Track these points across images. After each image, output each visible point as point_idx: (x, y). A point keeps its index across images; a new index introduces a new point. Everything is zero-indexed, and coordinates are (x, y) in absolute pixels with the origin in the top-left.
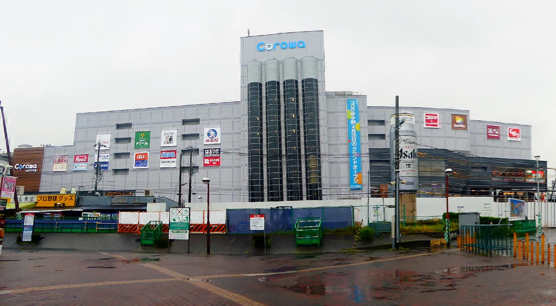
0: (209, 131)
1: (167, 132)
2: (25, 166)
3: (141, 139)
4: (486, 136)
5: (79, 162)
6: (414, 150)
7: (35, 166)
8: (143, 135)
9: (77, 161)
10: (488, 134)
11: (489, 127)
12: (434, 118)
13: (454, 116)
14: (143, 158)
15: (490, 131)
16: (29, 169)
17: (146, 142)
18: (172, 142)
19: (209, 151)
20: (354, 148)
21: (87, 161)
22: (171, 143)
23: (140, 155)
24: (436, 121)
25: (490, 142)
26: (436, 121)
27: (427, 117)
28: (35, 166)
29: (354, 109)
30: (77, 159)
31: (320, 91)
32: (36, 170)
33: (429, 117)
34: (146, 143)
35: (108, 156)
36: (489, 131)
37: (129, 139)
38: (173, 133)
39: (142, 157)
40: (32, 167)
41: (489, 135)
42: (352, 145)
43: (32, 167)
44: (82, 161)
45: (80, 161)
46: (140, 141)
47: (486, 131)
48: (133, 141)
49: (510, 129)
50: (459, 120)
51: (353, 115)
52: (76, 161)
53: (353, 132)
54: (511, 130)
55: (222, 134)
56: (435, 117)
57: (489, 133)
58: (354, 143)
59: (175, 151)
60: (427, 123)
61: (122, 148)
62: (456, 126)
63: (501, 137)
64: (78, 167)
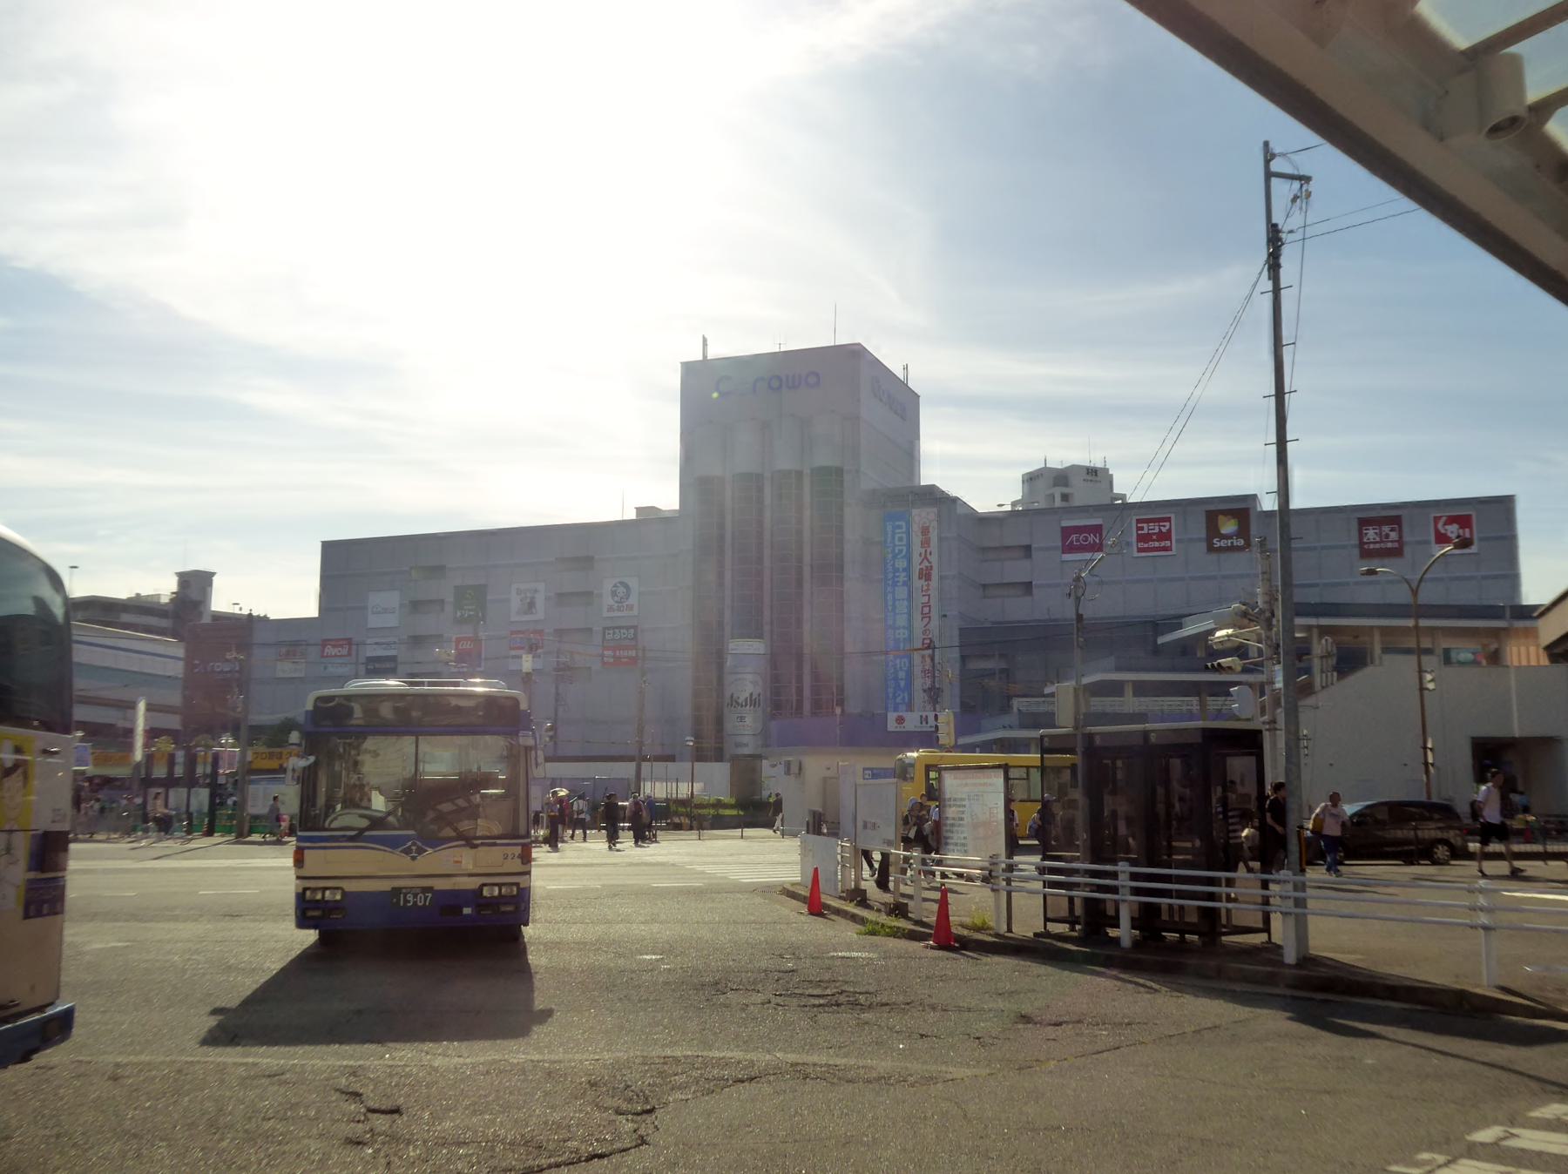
0: (615, 586)
4: (1356, 552)
8: (470, 594)
10: (1362, 544)
11: (1364, 523)
12: (1162, 528)
15: (1371, 534)
16: (221, 672)
18: (534, 611)
19: (614, 633)
22: (532, 613)
24: (1166, 536)
26: (1166, 536)
36: (1366, 534)
41: (1366, 546)
45: (333, 654)
47: (1355, 541)
49: (1437, 520)
50: (1229, 526)
56: (1164, 526)
57: (1365, 540)
62: (1217, 543)
63: (1407, 550)
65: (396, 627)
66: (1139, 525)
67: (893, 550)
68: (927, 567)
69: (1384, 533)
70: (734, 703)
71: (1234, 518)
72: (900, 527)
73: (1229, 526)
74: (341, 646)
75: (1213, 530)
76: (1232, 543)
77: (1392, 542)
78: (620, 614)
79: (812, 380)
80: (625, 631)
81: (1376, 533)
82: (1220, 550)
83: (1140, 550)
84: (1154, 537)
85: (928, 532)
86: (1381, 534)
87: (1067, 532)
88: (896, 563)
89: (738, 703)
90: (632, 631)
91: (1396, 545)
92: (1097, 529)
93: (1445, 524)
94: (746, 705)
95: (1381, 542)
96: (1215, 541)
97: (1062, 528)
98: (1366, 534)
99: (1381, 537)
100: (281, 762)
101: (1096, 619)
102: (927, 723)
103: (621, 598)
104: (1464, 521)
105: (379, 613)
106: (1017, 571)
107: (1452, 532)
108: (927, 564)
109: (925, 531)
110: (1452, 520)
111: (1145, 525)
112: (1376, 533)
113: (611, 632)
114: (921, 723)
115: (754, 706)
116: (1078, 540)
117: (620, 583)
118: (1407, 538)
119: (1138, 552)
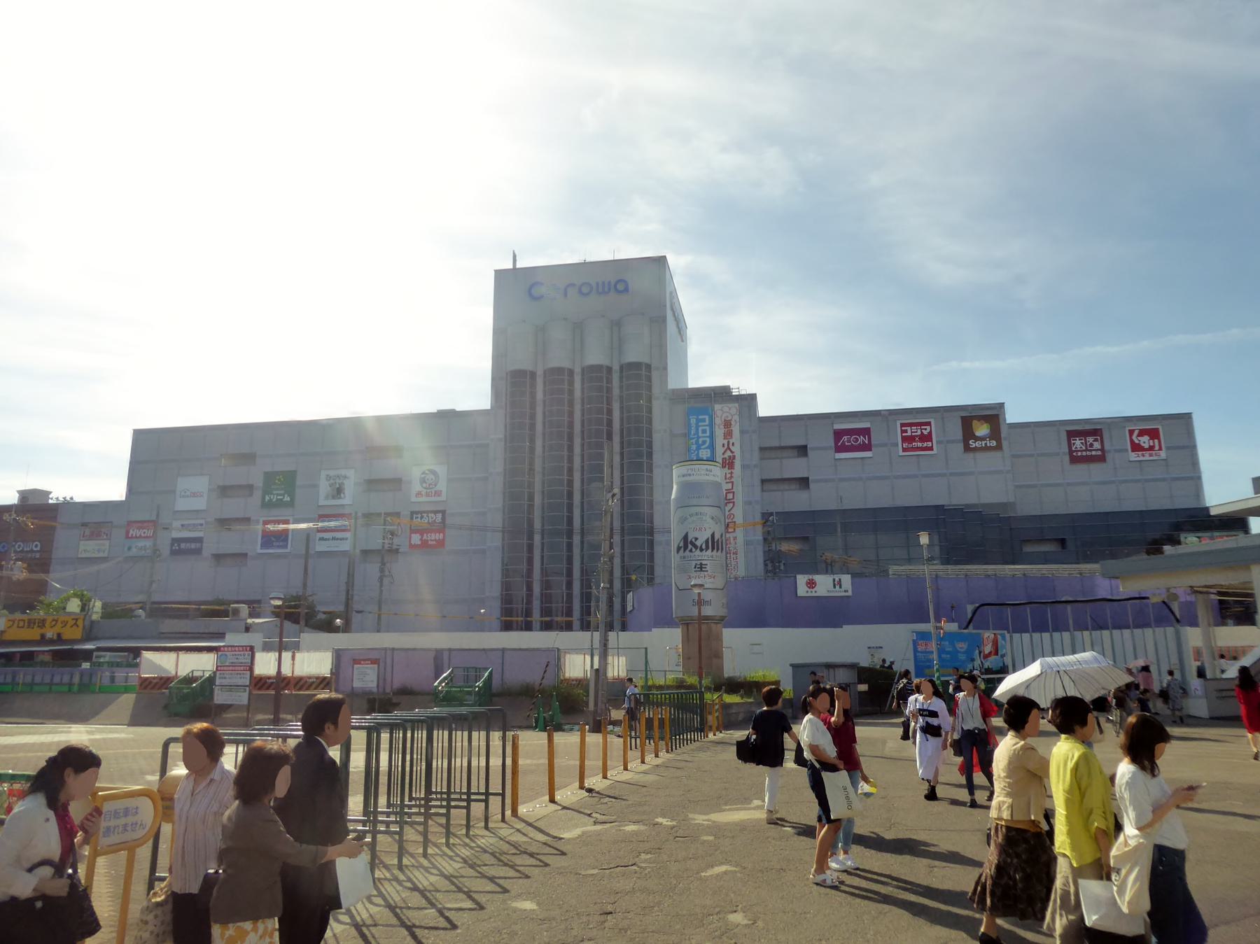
0: (423, 473)
1: (332, 473)
3: (277, 489)
4: (1067, 458)
5: (136, 537)
7: (36, 546)
8: (279, 480)
9: (132, 535)
10: (1071, 452)
11: (1072, 434)
15: (1078, 443)
17: (286, 496)
18: (342, 495)
22: (340, 498)
25: (1081, 470)
26: (928, 438)
27: (906, 431)
28: (36, 546)
30: (133, 530)
31: (656, 390)
32: (38, 556)
34: (287, 499)
35: (201, 525)
37: (250, 488)
38: (345, 477)
45: (138, 535)
46: (275, 492)
48: (258, 494)
50: (982, 430)
52: (130, 536)
56: (926, 429)
61: (233, 507)
65: (204, 510)
66: (903, 428)
67: (697, 443)
68: (730, 457)
70: (690, 546)
72: (704, 420)
75: (968, 434)
76: (986, 444)
79: (620, 287)
80: (433, 515)
82: (976, 449)
83: (904, 450)
85: (731, 424)
86: (1086, 443)
87: (838, 434)
88: (700, 453)
89: (696, 547)
90: (440, 516)
91: (1099, 453)
92: (866, 432)
94: (707, 548)
97: (834, 430)
98: (1074, 444)
99: (1086, 447)
100: (43, 631)
102: (840, 587)
104: (1154, 434)
105: (188, 496)
106: (796, 467)
107: (1144, 443)
108: (731, 454)
109: (727, 424)
110: (1142, 433)
111: (909, 429)
112: (1082, 443)
113: (419, 516)
114: (835, 587)
115: (713, 549)
116: (849, 441)
117: (428, 470)
118: (1107, 447)
119: (903, 451)
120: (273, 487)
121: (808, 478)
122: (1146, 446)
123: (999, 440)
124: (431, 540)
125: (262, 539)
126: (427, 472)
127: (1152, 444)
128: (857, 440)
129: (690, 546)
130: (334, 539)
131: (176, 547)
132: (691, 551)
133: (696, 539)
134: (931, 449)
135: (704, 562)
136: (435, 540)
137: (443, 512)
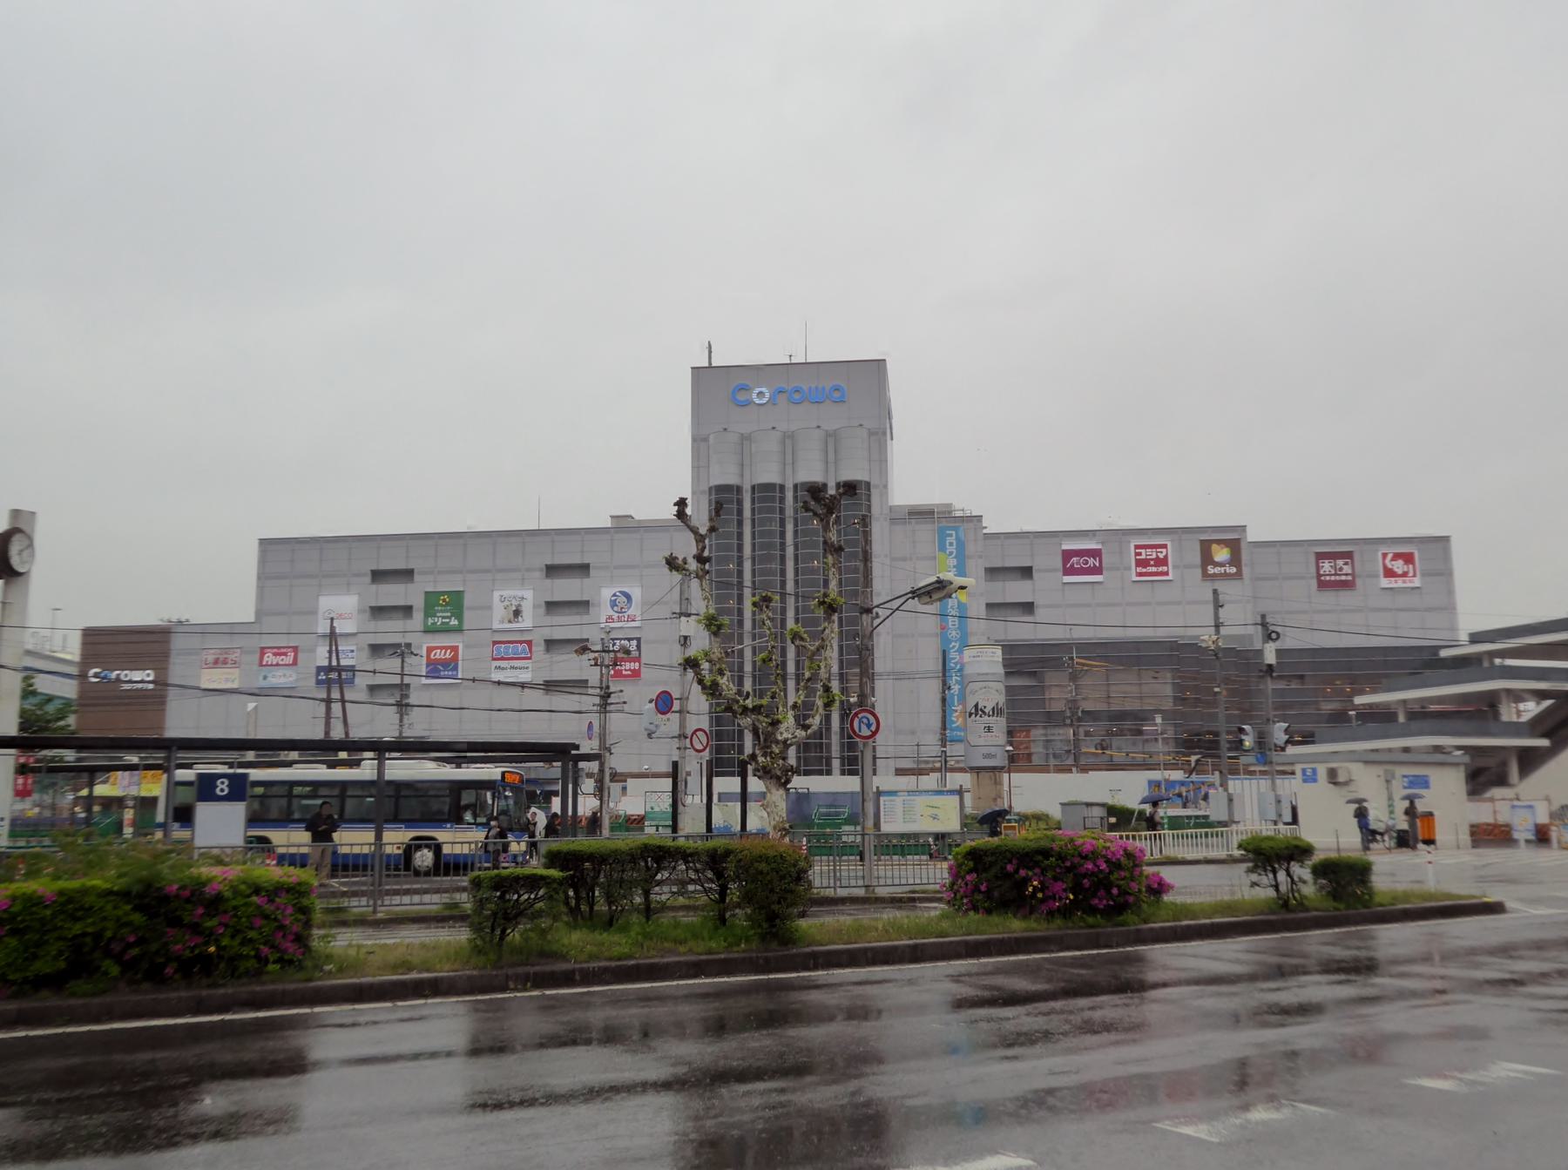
0: (614, 595)
1: (506, 593)
2: (118, 675)
3: (442, 611)
4: (1314, 583)
5: (272, 665)
6: (997, 704)
8: (444, 600)
9: (267, 662)
10: (1319, 575)
11: (1321, 556)
13: (1206, 547)
14: (447, 656)
15: (1327, 566)
16: (130, 682)
20: (953, 644)
21: (295, 663)
22: (518, 622)
23: (439, 651)
24: (1162, 562)
25: (1330, 598)
26: (1162, 562)
27: (1140, 554)
29: (955, 551)
31: (875, 510)
32: (151, 686)
33: (1144, 554)
34: (454, 622)
35: (352, 651)
36: (1323, 567)
37: (407, 610)
39: (445, 654)
40: (141, 677)
41: (1323, 578)
42: (950, 637)
43: (141, 677)
44: (281, 663)
45: (274, 663)
46: (438, 614)
47: (1313, 570)
48: (418, 616)
49: (1385, 555)
50: (1221, 554)
51: (952, 565)
52: (264, 663)
53: (951, 607)
54: (1390, 556)
55: (644, 603)
56: (1162, 552)
57: (1322, 572)
58: (954, 633)
59: (529, 643)
60: (1139, 569)
61: (391, 631)
62: (1211, 570)
63: (1359, 582)
64: (269, 679)
69: (1338, 567)
71: (1227, 547)
73: (1221, 554)
74: (285, 654)
75: (1207, 559)
76: (1225, 570)
77: (1346, 575)
78: (620, 624)
81: (1331, 566)
83: (1140, 574)
84: (1152, 563)
87: (1067, 555)
90: (634, 643)
91: (1350, 578)
92: (1095, 554)
93: (1392, 560)
95: (1336, 574)
96: (1209, 567)
97: (1063, 551)
98: (1323, 567)
99: (1336, 570)
101: (1073, 639)
103: (622, 608)
104: (1408, 558)
106: (1017, 591)
107: (1398, 568)
110: (1397, 556)
111: (1143, 551)
112: (1331, 566)
116: (1077, 564)
117: (620, 592)
120: (436, 608)
121: (1033, 603)
122: (1400, 572)
123: (1238, 565)
124: (626, 670)
125: (427, 666)
126: (618, 594)
127: (1406, 570)
128: (1087, 562)
129: (980, 713)
130: (512, 668)
131: (322, 677)
132: (981, 716)
133: (985, 707)
134: (1167, 574)
135: (991, 725)
136: (630, 670)
137: (639, 640)
